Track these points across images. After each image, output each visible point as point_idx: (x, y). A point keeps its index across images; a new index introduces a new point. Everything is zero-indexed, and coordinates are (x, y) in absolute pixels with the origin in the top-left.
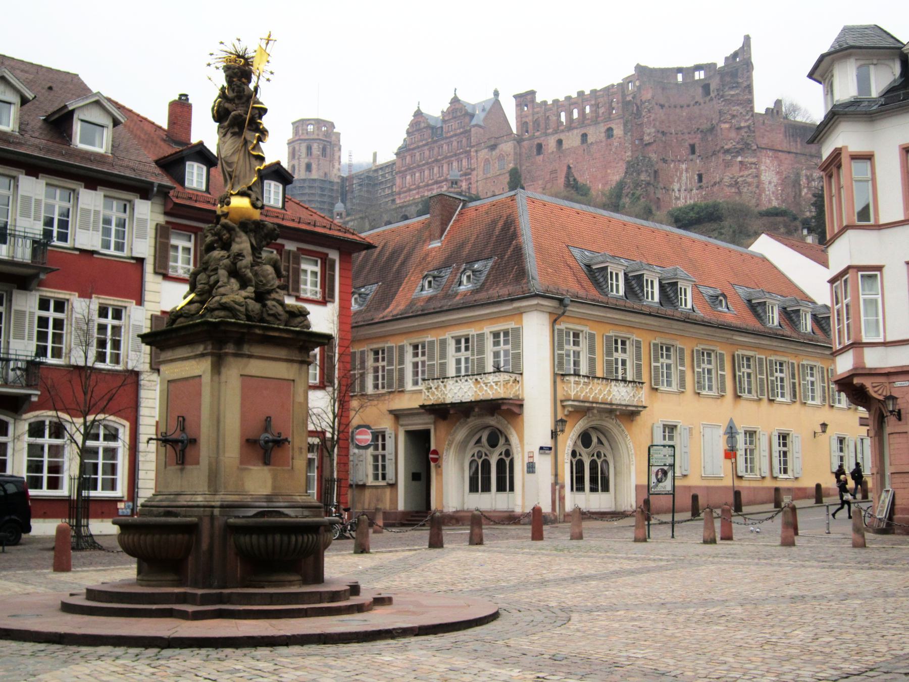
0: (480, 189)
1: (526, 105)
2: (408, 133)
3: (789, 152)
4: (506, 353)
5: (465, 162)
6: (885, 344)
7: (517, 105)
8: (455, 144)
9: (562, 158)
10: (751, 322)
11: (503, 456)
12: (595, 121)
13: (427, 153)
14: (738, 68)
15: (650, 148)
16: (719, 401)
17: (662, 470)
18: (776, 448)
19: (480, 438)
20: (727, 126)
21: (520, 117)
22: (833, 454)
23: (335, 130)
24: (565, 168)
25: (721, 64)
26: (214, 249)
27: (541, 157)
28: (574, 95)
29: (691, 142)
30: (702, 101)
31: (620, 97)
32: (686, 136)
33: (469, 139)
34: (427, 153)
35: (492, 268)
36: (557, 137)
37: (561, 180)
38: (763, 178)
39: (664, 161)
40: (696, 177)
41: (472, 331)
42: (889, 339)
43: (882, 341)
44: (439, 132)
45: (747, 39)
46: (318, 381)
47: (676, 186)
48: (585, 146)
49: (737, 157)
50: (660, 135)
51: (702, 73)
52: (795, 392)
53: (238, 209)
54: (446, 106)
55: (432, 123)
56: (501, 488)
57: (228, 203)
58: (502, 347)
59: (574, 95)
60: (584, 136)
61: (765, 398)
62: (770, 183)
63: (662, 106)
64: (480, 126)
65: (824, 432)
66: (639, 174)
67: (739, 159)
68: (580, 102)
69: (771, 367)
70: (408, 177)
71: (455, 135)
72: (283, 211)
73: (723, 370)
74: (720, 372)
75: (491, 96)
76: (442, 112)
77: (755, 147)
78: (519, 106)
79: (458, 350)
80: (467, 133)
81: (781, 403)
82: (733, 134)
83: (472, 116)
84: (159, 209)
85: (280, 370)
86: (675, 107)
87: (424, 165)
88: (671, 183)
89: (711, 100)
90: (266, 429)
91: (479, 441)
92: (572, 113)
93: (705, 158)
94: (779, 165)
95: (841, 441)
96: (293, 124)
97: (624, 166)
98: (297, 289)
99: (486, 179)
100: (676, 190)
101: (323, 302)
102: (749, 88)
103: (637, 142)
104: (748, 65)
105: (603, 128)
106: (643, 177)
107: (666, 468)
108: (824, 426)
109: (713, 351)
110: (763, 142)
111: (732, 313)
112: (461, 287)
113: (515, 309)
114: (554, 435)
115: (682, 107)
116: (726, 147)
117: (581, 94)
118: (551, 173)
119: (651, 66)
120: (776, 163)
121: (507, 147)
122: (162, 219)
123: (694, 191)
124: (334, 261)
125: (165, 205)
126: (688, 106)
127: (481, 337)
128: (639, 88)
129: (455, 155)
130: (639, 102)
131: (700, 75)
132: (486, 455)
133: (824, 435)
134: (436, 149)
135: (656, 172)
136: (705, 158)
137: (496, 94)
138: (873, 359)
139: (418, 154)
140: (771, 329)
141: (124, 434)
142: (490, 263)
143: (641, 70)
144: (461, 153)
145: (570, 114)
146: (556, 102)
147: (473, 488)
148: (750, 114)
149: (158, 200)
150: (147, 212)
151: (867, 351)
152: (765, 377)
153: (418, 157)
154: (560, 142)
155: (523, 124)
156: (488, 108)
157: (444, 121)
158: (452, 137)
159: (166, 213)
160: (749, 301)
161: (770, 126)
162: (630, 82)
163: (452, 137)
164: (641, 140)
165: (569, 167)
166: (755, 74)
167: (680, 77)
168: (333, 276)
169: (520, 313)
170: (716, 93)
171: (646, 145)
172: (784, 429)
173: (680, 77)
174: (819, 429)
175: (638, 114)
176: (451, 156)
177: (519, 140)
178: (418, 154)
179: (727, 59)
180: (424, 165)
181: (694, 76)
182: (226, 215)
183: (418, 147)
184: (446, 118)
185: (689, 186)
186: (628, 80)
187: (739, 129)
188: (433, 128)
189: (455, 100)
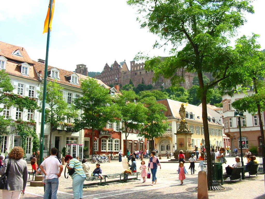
0: (122, 83)
2: (104, 69)
5: (118, 76)
6: (233, 128)
8: (115, 72)
13: (109, 73)
21: (132, 67)
23: (86, 67)
27: (136, 76)
37: (141, 81)
38: (186, 82)
42: (234, 127)
43: (232, 128)
54: (113, 63)
62: (188, 83)
70: (104, 79)
75: (124, 61)
78: (131, 64)
83: (120, 66)
88: (166, 83)
96: (77, 65)
106: (160, 81)
108: (215, 139)
129: (115, 74)
137: (125, 60)
138: (231, 130)
141: (119, 142)
146: (140, 63)
151: (230, 129)
153: (106, 74)
154: (141, 73)
158: (115, 70)
163: (115, 70)
165: (143, 78)
183: (106, 72)
189: (116, 62)
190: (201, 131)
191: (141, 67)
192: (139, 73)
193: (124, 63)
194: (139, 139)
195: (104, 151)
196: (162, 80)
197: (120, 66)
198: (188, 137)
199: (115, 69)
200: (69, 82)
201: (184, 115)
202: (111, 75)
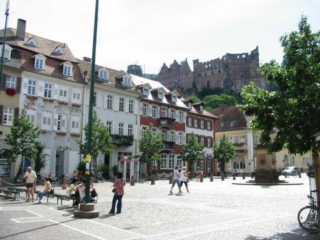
0: (183, 85)
5: (178, 78)
12: (216, 68)
14: (255, 54)
18: (292, 159)
20: (252, 70)
21: (194, 66)
24: (207, 81)
25: (250, 54)
27: (200, 78)
28: (210, 61)
33: (179, 72)
36: (205, 72)
45: (257, 47)
47: (238, 86)
54: (172, 62)
56: (241, 168)
59: (210, 61)
60: (213, 73)
82: (253, 72)
93: (246, 79)
101: (211, 130)
104: (258, 54)
105: (218, 70)
106: (229, 84)
114: (254, 157)
119: (231, 53)
121: (190, 75)
128: (228, 59)
131: (244, 56)
136: (246, 79)
137: (186, 59)
142: (237, 120)
143: (228, 54)
154: (206, 74)
155: (195, 68)
164: (228, 73)
166: (259, 56)
167: (238, 56)
173: (238, 56)
175: (227, 67)
177: (194, 72)
179: (251, 52)
186: (223, 57)
189: (175, 61)
191: (206, 66)
192: (203, 74)
193: (185, 63)
195: (164, 168)
196: (232, 83)
200: (121, 84)
202: (170, 77)
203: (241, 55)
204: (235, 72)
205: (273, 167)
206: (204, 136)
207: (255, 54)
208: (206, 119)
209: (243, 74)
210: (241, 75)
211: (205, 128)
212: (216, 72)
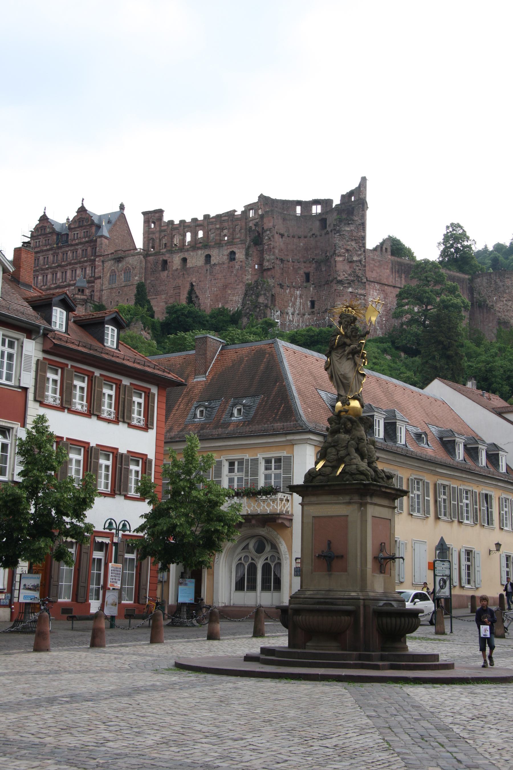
0: (104, 298)
1: (154, 223)
2: (33, 236)
3: (394, 287)
4: (277, 476)
5: (88, 271)
7: (145, 222)
8: (80, 252)
9: (186, 276)
10: (441, 455)
11: (269, 561)
12: (219, 244)
13: (51, 258)
15: (269, 273)
16: (425, 521)
17: (443, 579)
19: (248, 545)
20: (341, 259)
22: (502, 569)
25: (337, 201)
26: (340, 432)
27: (165, 273)
28: (201, 218)
29: (307, 271)
30: (318, 233)
31: (244, 224)
32: (302, 265)
33: (94, 248)
34: (51, 258)
35: (260, 404)
39: (281, 286)
40: (309, 304)
41: (247, 456)
44: (64, 238)
45: (364, 180)
46: (109, 490)
47: (290, 310)
48: (208, 267)
49: (348, 288)
50: (278, 262)
51: (319, 207)
52: (477, 515)
53: (354, 408)
54: (72, 214)
55: (57, 229)
56: (266, 587)
57: (349, 404)
58: (273, 471)
59: (201, 218)
60: (208, 257)
61: (456, 520)
63: (282, 235)
64: (106, 238)
65: (498, 550)
66: (258, 296)
67: (350, 290)
68: (206, 223)
69: (461, 495)
71: (81, 243)
72: (117, 351)
73: (428, 496)
74: (426, 498)
75: (118, 209)
76: (68, 219)
77: (365, 280)
79: (231, 470)
80: (93, 243)
81: (467, 525)
82: (347, 267)
84: (40, 347)
85: (384, 512)
86: (293, 237)
87: (47, 269)
88: (286, 307)
89: (327, 233)
90: (381, 551)
91: (246, 547)
92: (197, 234)
94: (385, 298)
95: (508, 558)
97: (244, 288)
98: (130, 418)
99: (112, 289)
100: (290, 314)
101: (146, 428)
102: (363, 226)
103: (256, 267)
105: (226, 251)
106: (261, 300)
107: (445, 578)
108: (498, 545)
109: (421, 480)
110: (371, 275)
111: (431, 450)
112: (233, 419)
113: (287, 441)
115: (299, 237)
116: (339, 278)
117: (206, 217)
118: (175, 288)
119: (273, 197)
120: (382, 296)
122: (41, 356)
123: (307, 316)
124: (154, 395)
125: (44, 344)
126: (305, 237)
127: (255, 461)
128: (262, 217)
129: (80, 262)
130: (260, 230)
131: (316, 209)
132: (252, 559)
133: (498, 553)
134: (60, 255)
135: (273, 295)
136: (318, 286)
137: (122, 207)
139: (41, 258)
140: (458, 462)
142: (258, 400)
144: (86, 261)
145: (194, 235)
146: (182, 222)
147: (240, 586)
148: (362, 249)
149: (40, 340)
150: (32, 349)
152: (456, 503)
156: (113, 221)
157: (70, 228)
158: (77, 245)
159: (44, 351)
160: (441, 438)
161: (379, 261)
162: (252, 209)
163: (77, 245)
165: (192, 285)
167: (298, 209)
168: (154, 407)
169: (292, 444)
170: (332, 227)
171: (265, 270)
172: (469, 546)
173: (298, 209)
174: (494, 548)
176: (76, 263)
178: (41, 258)
179: (343, 196)
180: (47, 269)
181: (311, 210)
182: (346, 411)
184: (72, 226)
185: (302, 311)
186: (249, 208)
187: (352, 262)
188: (58, 234)
189: (82, 210)
190: (436, 501)
191: (189, 237)
192: (176, 261)
194: (110, 524)
197: (99, 227)
198: (375, 510)
199: (77, 241)
201: (351, 375)
203: (306, 205)
204: (282, 260)
205: (377, 585)
206: (114, 451)
207: (354, 204)
208: (126, 382)
209: (311, 270)
210: (301, 272)
211: (122, 416)
212: (219, 256)
